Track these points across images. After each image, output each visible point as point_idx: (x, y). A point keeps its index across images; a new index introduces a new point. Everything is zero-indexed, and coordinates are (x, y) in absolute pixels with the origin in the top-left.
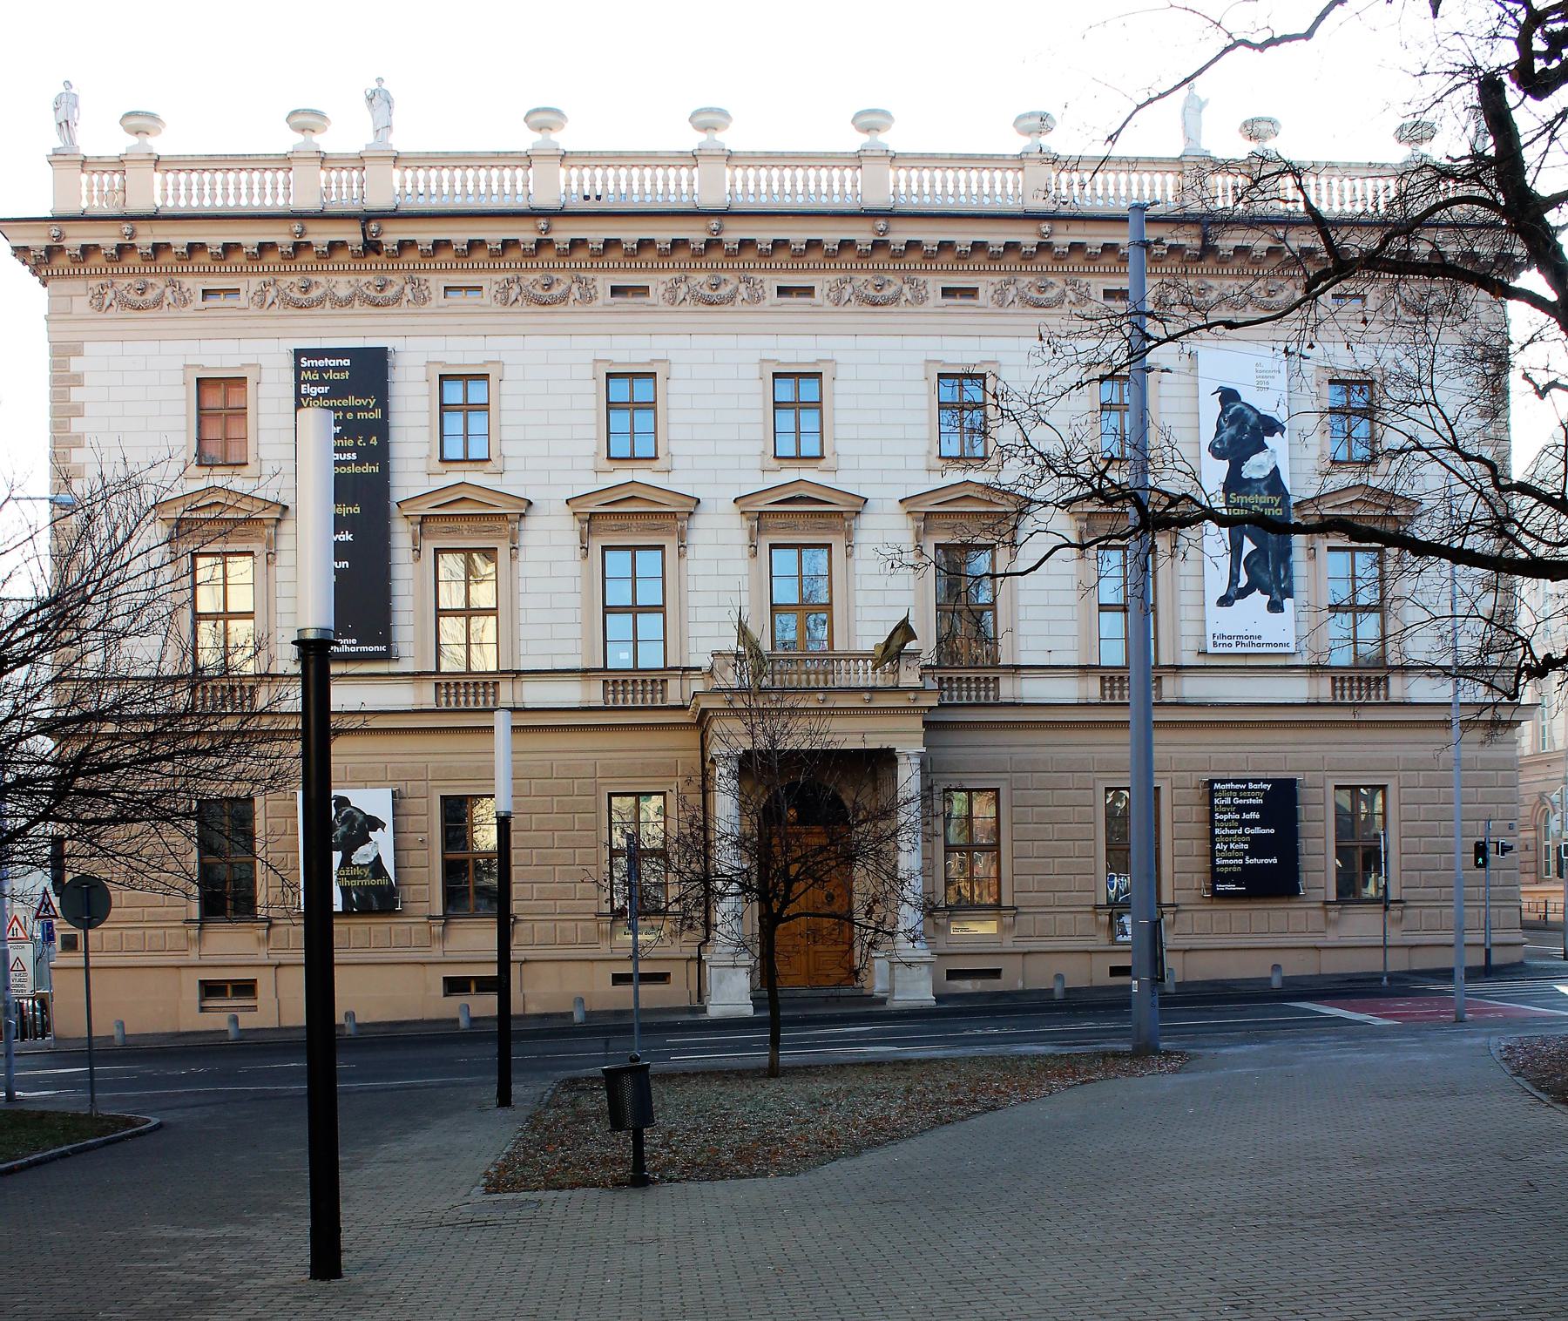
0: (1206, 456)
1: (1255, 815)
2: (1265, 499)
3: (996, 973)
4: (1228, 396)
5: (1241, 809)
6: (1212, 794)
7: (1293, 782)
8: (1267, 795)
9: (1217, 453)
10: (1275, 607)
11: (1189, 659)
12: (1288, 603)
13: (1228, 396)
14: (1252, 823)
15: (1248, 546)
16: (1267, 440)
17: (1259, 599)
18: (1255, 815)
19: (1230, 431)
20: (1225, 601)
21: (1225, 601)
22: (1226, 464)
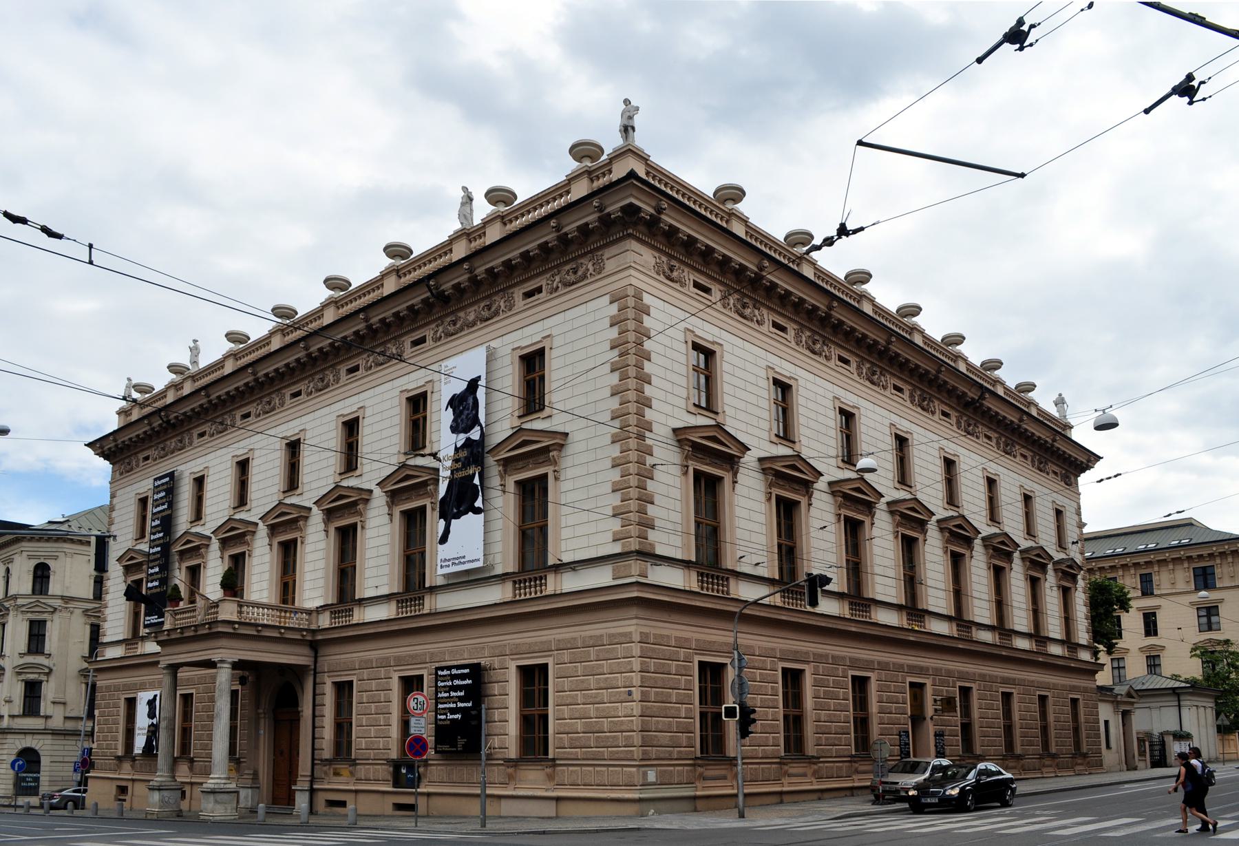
11: (440, 581)
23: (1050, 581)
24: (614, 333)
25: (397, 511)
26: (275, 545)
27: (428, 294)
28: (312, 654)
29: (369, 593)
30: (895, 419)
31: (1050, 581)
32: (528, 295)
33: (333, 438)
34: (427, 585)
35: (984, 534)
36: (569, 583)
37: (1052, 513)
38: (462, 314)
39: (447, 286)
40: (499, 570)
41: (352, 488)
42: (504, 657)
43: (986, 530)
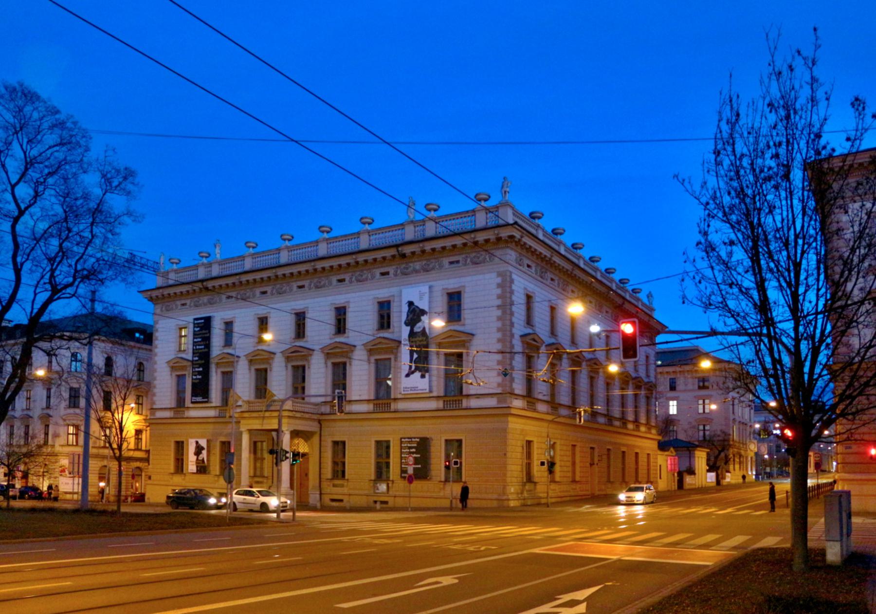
0: (404, 326)
1: (414, 450)
2: (420, 339)
3: (341, 501)
4: (411, 304)
5: (410, 448)
6: (401, 442)
7: (427, 439)
8: (418, 443)
9: (407, 324)
10: (423, 376)
12: (427, 375)
13: (411, 304)
14: (413, 453)
15: (415, 356)
16: (422, 318)
17: (418, 374)
18: (414, 450)
19: (411, 316)
20: (407, 375)
21: (407, 375)
22: (409, 328)
23: (565, 367)
24: (499, 291)
25: (373, 359)
26: (290, 368)
27: (396, 253)
28: (319, 425)
29: (354, 398)
30: (526, 283)
31: (565, 367)
32: (451, 263)
33: (330, 317)
34: (392, 397)
35: (547, 343)
36: (474, 403)
37: (548, 309)
38: (411, 265)
39: (408, 250)
40: (435, 394)
41: (342, 343)
42: (439, 434)
43: (548, 340)
